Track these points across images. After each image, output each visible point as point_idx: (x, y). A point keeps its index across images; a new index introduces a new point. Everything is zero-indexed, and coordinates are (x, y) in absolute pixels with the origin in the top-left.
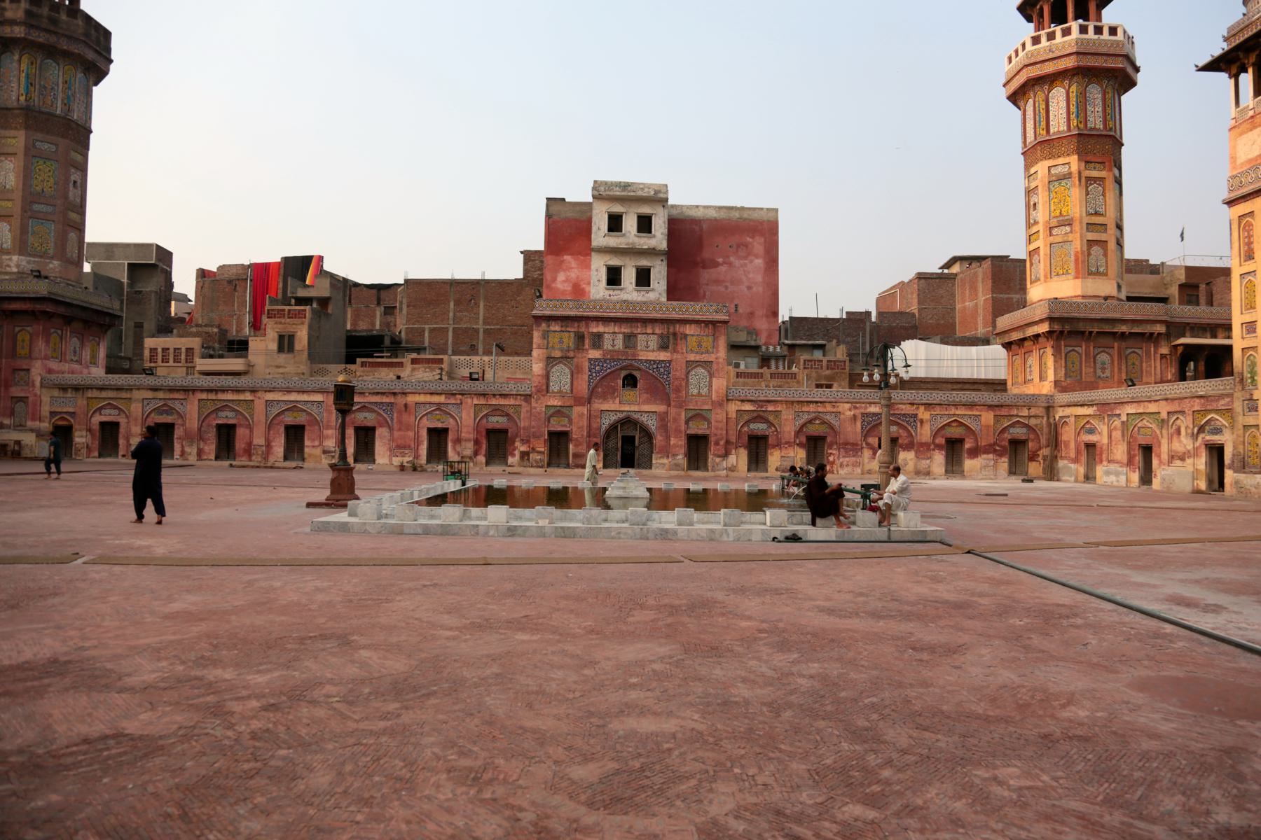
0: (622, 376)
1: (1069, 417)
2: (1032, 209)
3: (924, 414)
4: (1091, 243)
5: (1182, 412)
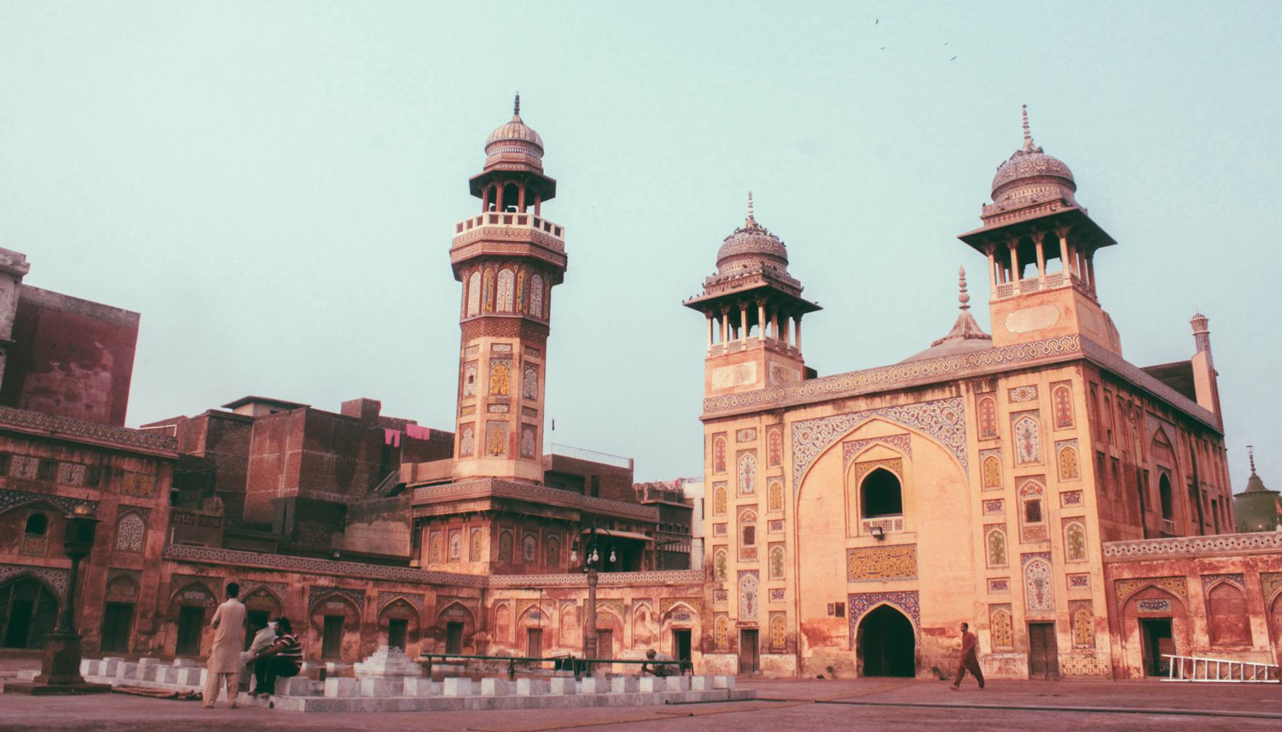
0: (28, 515)
1: (508, 600)
2: (467, 381)
3: (372, 591)
4: (525, 426)
5: (649, 599)
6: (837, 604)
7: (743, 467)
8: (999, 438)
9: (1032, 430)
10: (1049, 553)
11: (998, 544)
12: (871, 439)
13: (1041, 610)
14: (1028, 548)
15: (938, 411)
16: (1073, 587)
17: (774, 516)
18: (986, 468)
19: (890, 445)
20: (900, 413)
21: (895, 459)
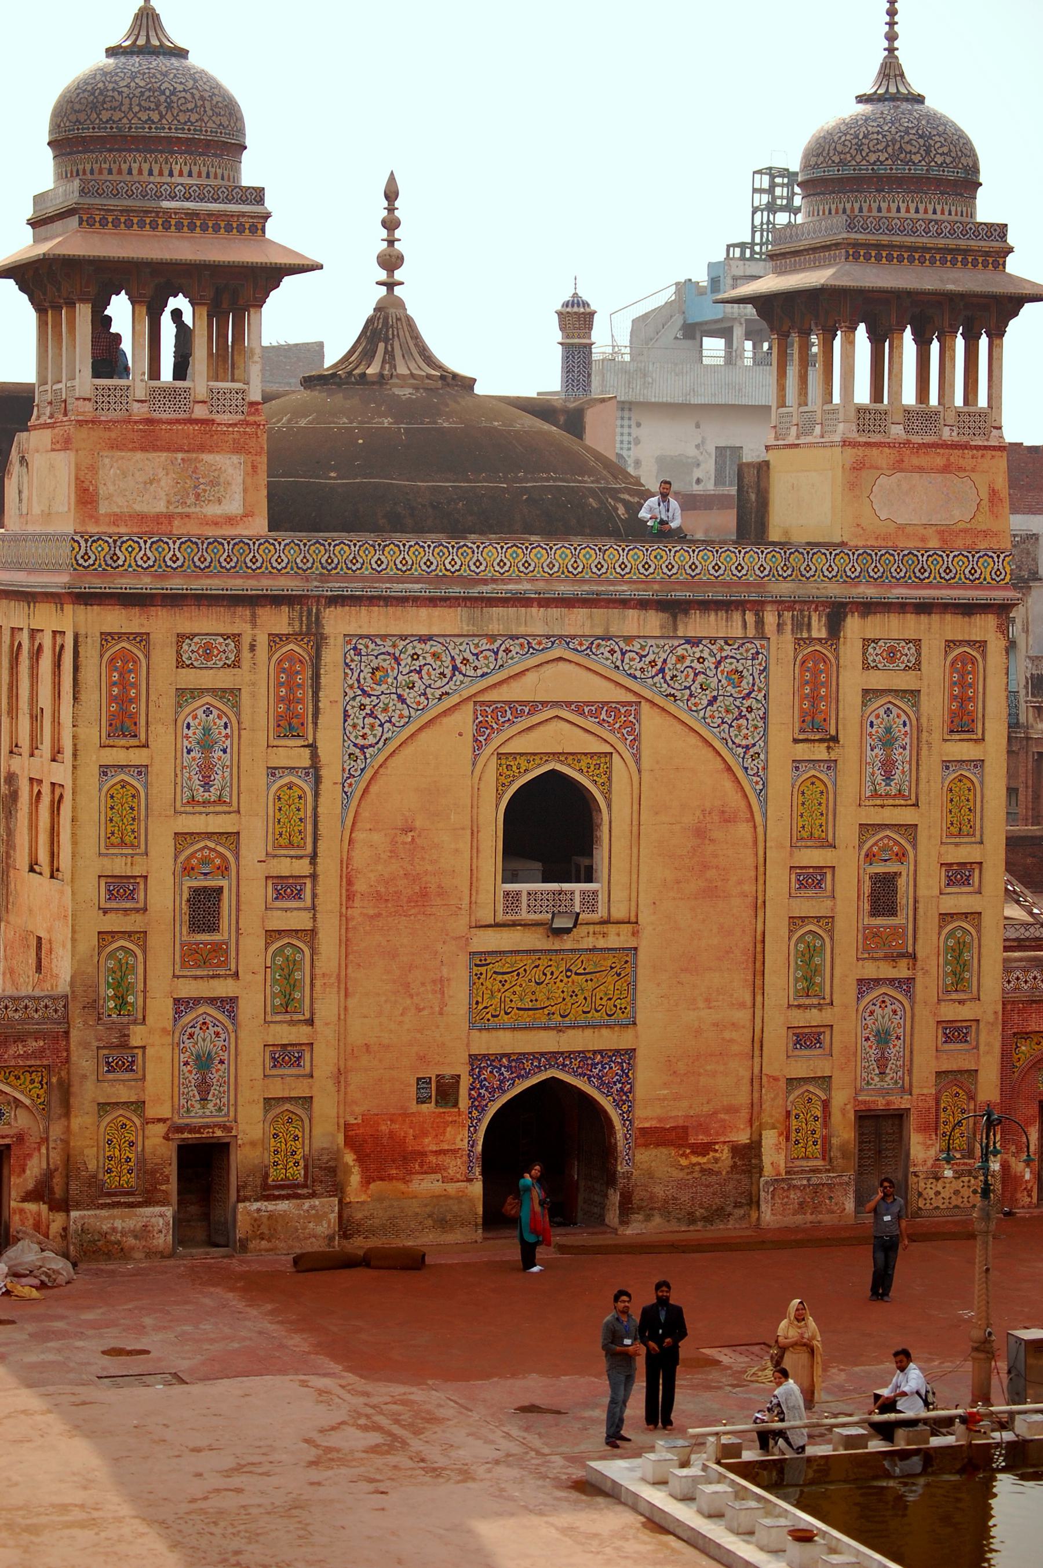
6: (438, 1076)
7: (195, 733)
8: (835, 739)
9: (898, 730)
10: (910, 981)
11: (811, 957)
12: (544, 703)
13: (882, 1088)
14: (870, 970)
15: (710, 663)
16: (947, 1046)
17: (285, 867)
18: (801, 799)
19: (589, 723)
20: (623, 654)
21: (592, 755)
